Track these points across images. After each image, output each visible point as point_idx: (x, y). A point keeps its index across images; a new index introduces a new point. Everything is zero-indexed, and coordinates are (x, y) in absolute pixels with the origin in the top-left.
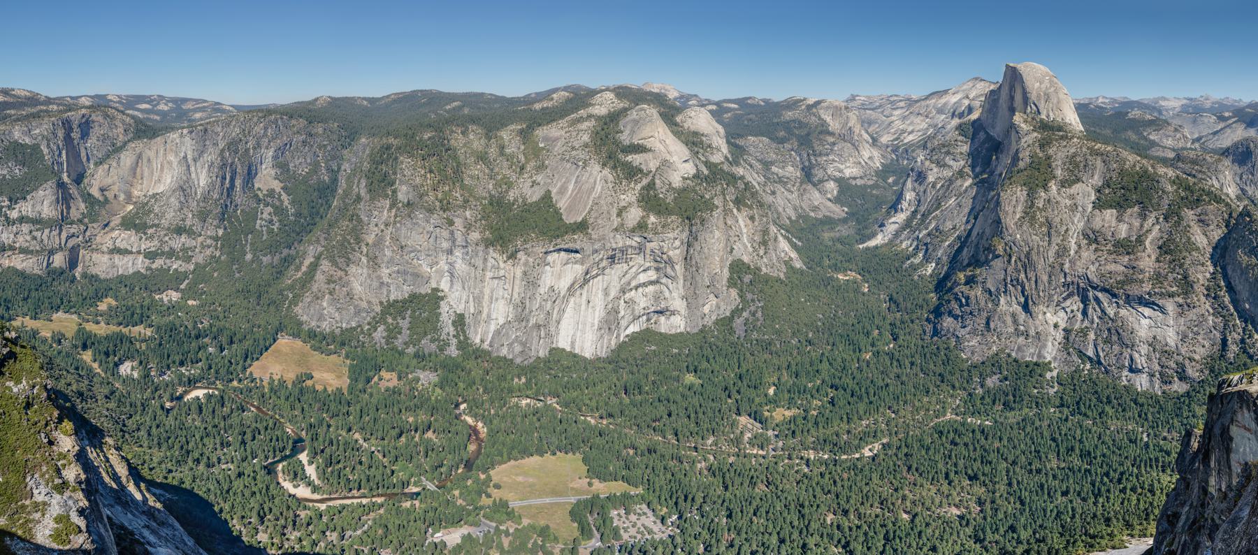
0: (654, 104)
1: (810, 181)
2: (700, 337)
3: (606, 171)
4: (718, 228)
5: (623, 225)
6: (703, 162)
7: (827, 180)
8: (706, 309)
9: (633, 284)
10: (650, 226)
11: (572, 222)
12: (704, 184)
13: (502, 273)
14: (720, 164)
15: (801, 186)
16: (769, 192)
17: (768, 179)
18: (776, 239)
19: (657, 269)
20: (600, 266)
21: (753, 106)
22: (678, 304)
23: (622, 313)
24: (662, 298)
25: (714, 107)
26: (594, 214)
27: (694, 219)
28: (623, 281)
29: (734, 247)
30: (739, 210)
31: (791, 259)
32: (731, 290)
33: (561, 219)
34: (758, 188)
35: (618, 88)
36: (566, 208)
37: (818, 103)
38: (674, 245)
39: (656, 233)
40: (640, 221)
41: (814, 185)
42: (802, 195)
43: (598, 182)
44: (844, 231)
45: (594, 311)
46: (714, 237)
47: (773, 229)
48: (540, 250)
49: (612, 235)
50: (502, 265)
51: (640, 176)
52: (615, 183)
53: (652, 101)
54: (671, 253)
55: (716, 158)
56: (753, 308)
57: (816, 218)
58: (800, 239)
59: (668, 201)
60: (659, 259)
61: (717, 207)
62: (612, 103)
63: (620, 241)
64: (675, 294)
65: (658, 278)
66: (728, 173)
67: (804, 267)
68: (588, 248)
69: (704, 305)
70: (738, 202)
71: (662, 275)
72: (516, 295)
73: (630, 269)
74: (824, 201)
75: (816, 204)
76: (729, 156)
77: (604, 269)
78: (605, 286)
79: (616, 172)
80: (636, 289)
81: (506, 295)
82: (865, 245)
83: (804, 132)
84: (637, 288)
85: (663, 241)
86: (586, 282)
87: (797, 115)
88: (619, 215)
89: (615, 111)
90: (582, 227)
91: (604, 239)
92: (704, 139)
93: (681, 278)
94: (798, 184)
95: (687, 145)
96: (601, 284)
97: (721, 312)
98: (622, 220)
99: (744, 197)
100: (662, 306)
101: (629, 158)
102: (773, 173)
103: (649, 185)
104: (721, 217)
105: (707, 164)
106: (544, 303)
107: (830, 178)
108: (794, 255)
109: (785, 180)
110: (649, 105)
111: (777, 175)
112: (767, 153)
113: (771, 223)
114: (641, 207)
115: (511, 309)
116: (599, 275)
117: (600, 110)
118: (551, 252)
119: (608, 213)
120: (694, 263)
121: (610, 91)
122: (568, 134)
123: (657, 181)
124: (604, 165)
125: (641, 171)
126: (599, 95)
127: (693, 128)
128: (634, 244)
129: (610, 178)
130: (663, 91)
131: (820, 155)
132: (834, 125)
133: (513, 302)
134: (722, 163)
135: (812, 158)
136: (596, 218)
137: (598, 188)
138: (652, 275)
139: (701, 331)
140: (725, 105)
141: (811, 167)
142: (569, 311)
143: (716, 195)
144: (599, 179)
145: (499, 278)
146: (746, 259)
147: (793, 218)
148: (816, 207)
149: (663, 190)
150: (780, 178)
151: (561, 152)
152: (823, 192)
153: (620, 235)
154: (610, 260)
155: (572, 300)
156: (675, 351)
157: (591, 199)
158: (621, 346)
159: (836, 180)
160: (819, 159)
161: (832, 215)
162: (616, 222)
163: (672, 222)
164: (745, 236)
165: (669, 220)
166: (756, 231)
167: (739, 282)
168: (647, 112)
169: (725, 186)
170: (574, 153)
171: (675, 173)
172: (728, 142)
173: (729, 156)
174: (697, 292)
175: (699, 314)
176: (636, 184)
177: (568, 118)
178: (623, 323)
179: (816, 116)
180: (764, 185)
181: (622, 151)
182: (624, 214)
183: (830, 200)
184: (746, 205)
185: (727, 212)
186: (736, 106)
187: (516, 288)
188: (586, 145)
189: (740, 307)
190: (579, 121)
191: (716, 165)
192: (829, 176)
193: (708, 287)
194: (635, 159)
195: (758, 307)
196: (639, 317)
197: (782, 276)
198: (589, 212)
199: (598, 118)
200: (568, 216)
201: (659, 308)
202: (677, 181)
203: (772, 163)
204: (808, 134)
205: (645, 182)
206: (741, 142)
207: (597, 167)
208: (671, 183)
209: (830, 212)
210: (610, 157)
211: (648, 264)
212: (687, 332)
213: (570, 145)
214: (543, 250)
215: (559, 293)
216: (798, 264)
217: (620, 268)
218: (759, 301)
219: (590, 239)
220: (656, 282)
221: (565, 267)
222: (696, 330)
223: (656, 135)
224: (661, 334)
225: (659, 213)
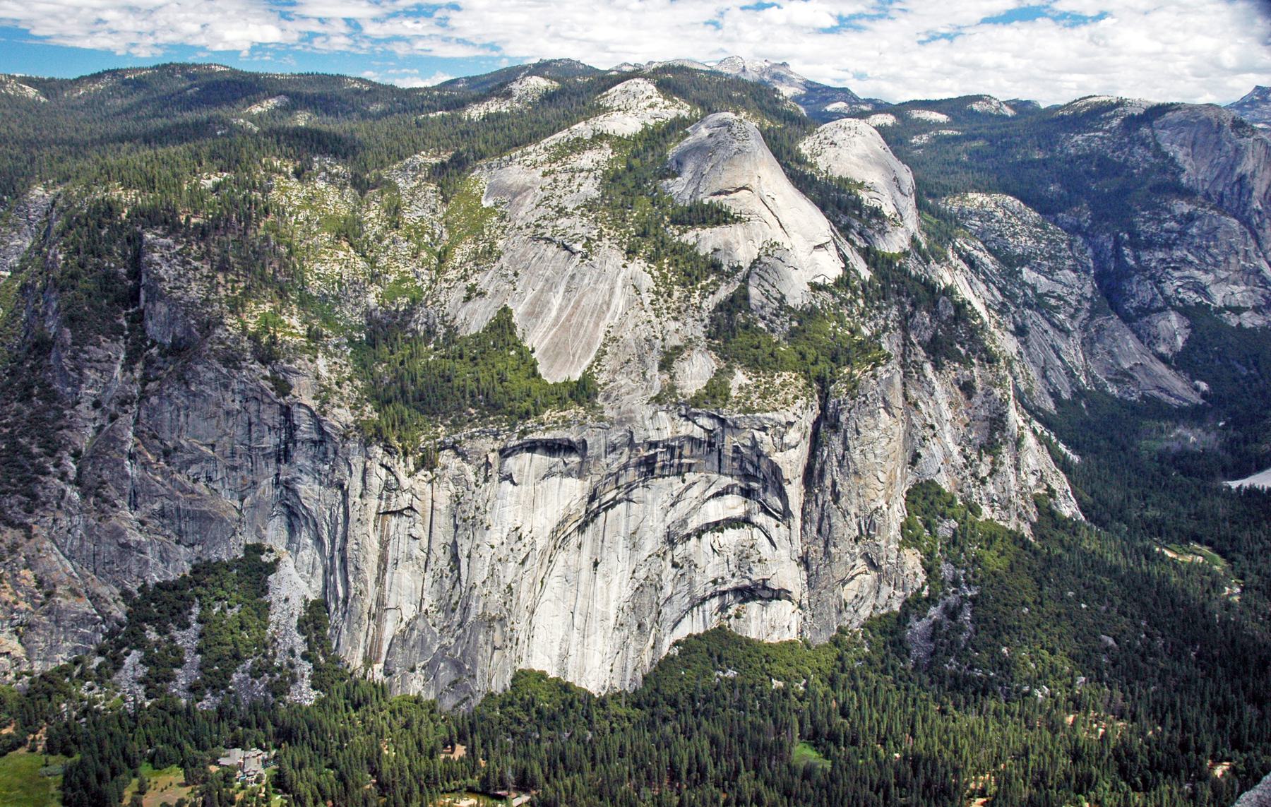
0: (747, 109)
1: (1115, 308)
2: (832, 656)
3: (638, 266)
4: (887, 407)
5: (673, 389)
6: (859, 250)
7: (1160, 310)
8: (848, 593)
9: (694, 523)
10: (734, 393)
11: (560, 381)
12: (861, 302)
13: (404, 500)
14: (898, 257)
15: (1091, 318)
16: (1012, 327)
17: (1012, 297)
18: (1019, 442)
19: (747, 493)
20: (622, 482)
21: (986, 116)
22: (789, 576)
23: (668, 590)
24: (755, 558)
25: (889, 120)
26: (609, 363)
27: (833, 382)
28: (673, 515)
29: (922, 451)
30: (937, 367)
31: (1051, 492)
32: (906, 551)
33: (535, 374)
34: (986, 318)
35: (667, 68)
36: (546, 350)
37: (1158, 111)
38: (787, 440)
39: (748, 410)
40: (710, 381)
41: (1126, 319)
42: (1092, 341)
43: (618, 291)
44: (1193, 437)
45: (608, 584)
46: (876, 426)
47: (1015, 417)
48: (487, 446)
49: (649, 411)
50: (406, 482)
51: (713, 278)
52: (657, 293)
53: (742, 102)
54: (777, 457)
55: (893, 244)
56: (952, 599)
57: (1121, 402)
58: (1076, 448)
59: (775, 338)
60: (751, 470)
61: (888, 357)
62: (651, 106)
63: (666, 427)
64: (783, 553)
65: (748, 512)
66: (917, 279)
67: (1081, 517)
68: (596, 441)
69: (844, 582)
70: (938, 351)
71: (757, 506)
72: (438, 551)
73: (687, 489)
74: (1146, 361)
75: (1126, 366)
76: (922, 238)
77: (630, 487)
78: (632, 528)
79: (660, 269)
80: (699, 537)
81: (416, 552)
82: (1246, 483)
83: (1108, 186)
84: (699, 533)
85: (764, 429)
86: (590, 517)
87: (1097, 143)
88: (665, 365)
89: (657, 126)
90: (582, 391)
91: (630, 420)
92: (864, 195)
93: (797, 513)
94: (1083, 315)
95: (823, 209)
96: (623, 523)
97: (881, 601)
98: (672, 378)
99: (952, 338)
100: (754, 578)
101: (689, 237)
102: (1024, 284)
103: (732, 299)
104: (898, 379)
105: (869, 255)
106: (498, 566)
107: (1168, 304)
108: (1060, 483)
109: (1053, 302)
110: (737, 113)
111: (1034, 288)
112: (1014, 235)
113: (1012, 403)
114: (714, 349)
115: (429, 581)
116: (619, 502)
117: (625, 124)
118: (514, 451)
119: (642, 360)
120: (828, 482)
121: (645, 77)
122: (549, 179)
123: (754, 292)
124: (631, 253)
125: (715, 267)
126: (620, 87)
127: (838, 171)
128: (698, 433)
129: (647, 282)
130: (766, 78)
131: (1150, 244)
132: (1193, 170)
133: (432, 565)
134: (905, 254)
135: (1126, 251)
136: (615, 372)
137: (619, 302)
138: (734, 506)
139: (836, 642)
140: (916, 114)
141: (1125, 273)
142: (554, 582)
143: (885, 328)
144: (620, 283)
145: (400, 513)
146: (945, 483)
147: (1066, 395)
148: (1125, 373)
149: (767, 312)
150: (1040, 296)
151: (533, 220)
152: (1148, 339)
153: (668, 411)
154: (643, 469)
155: (560, 557)
156: (777, 684)
157: (603, 328)
158: (664, 665)
159: (1186, 311)
160: (1145, 256)
161: (1165, 397)
162: (658, 380)
163: (783, 385)
164: (948, 427)
165: (778, 381)
166: (974, 418)
167: (926, 533)
168: (735, 130)
169: (908, 308)
170: (563, 222)
171: (794, 274)
172: (920, 206)
173: (922, 238)
174: (833, 550)
175: (833, 601)
176: (703, 297)
177: (550, 141)
178: (669, 613)
179: (1147, 147)
180: (1000, 312)
181: (674, 222)
182: (675, 364)
183: (1162, 358)
184: (956, 357)
185: (910, 370)
186: (942, 118)
187: (437, 532)
188: (590, 206)
189: (925, 593)
190: (573, 149)
191: (889, 260)
192: (1167, 299)
193: (856, 540)
194: (707, 239)
195: (964, 598)
196: (704, 600)
197: (1026, 531)
198: (598, 359)
199: (619, 142)
200: (551, 366)
201: (747, 582)
202: (797, 295)
203: (1024, 260)
204: (1123, 192)
205: (724, 292)
206: (951, 204)
207: (618, 258)
208: (783, 297)
209: (1161, 389)
210: (644, 234)
211: (727, 481)
212: (805, 641)
213: (554, 203)
214: (497, 445)
215: (533, 543)
216: (1068, 509)
217: (667, 486)
218: (968, 584)
219: (601, 419)
220: (745, 521)
221: (545, 483)
222: (823, 639)
223: (754, 184)
224: (749, 641)
225: (754, 365)
